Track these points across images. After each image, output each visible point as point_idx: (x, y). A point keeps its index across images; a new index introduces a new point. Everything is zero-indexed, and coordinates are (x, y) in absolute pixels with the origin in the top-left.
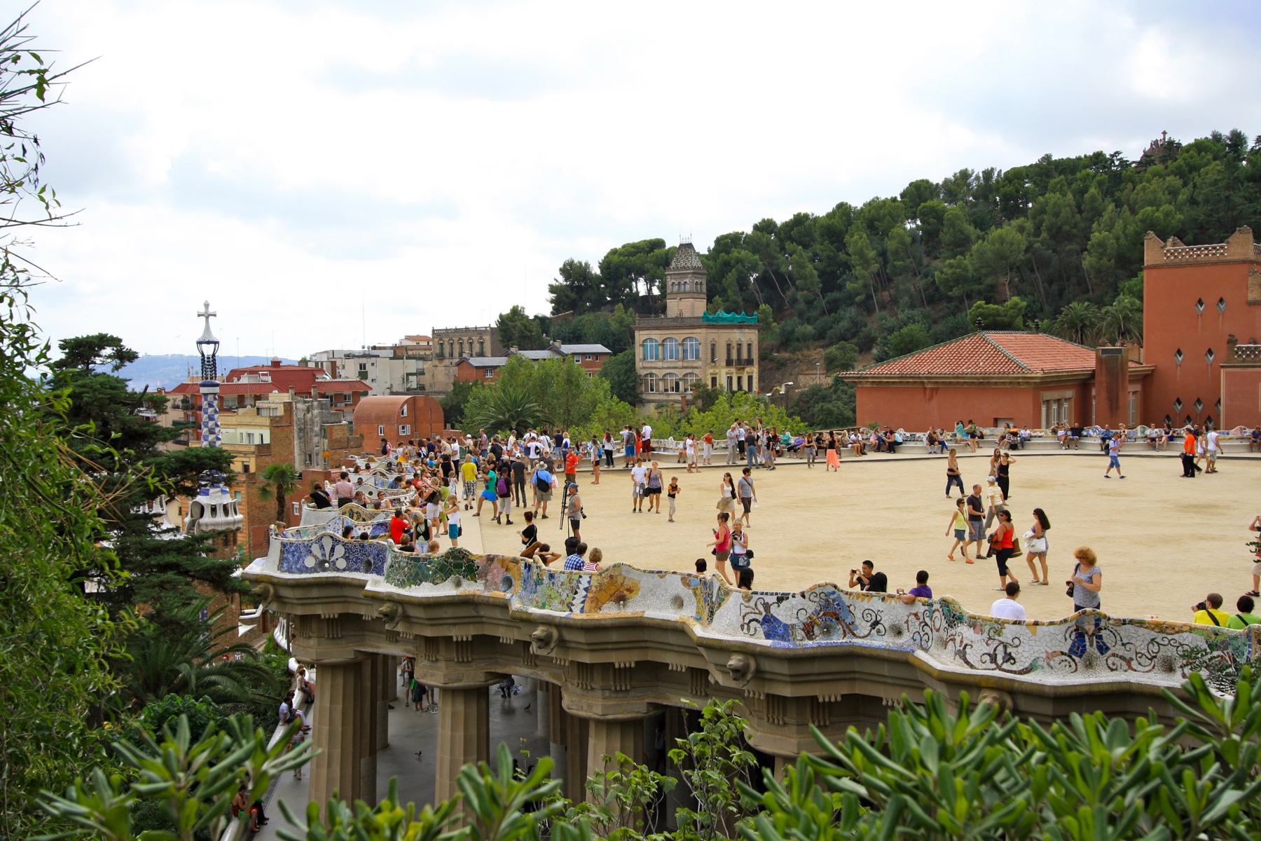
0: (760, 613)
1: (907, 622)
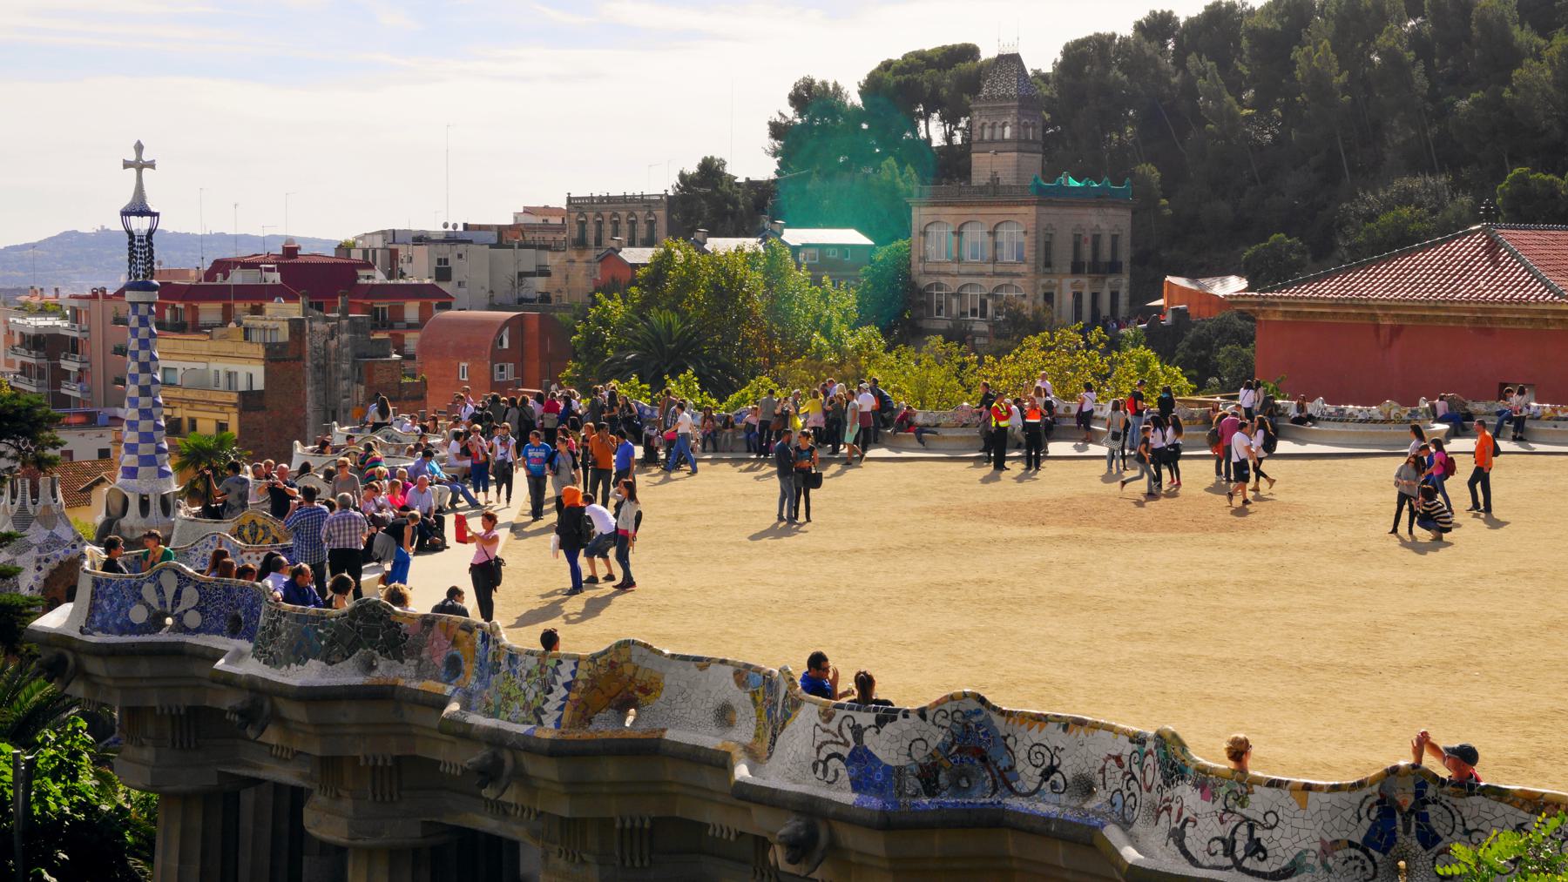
0: (846, 744)
1: (1103, 770)
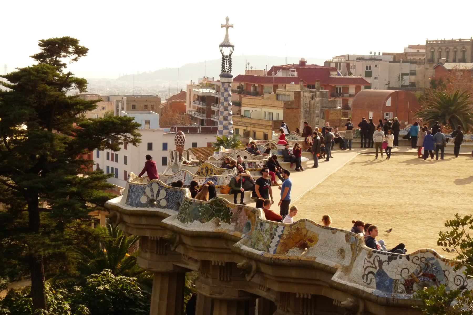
0: (376, 268)
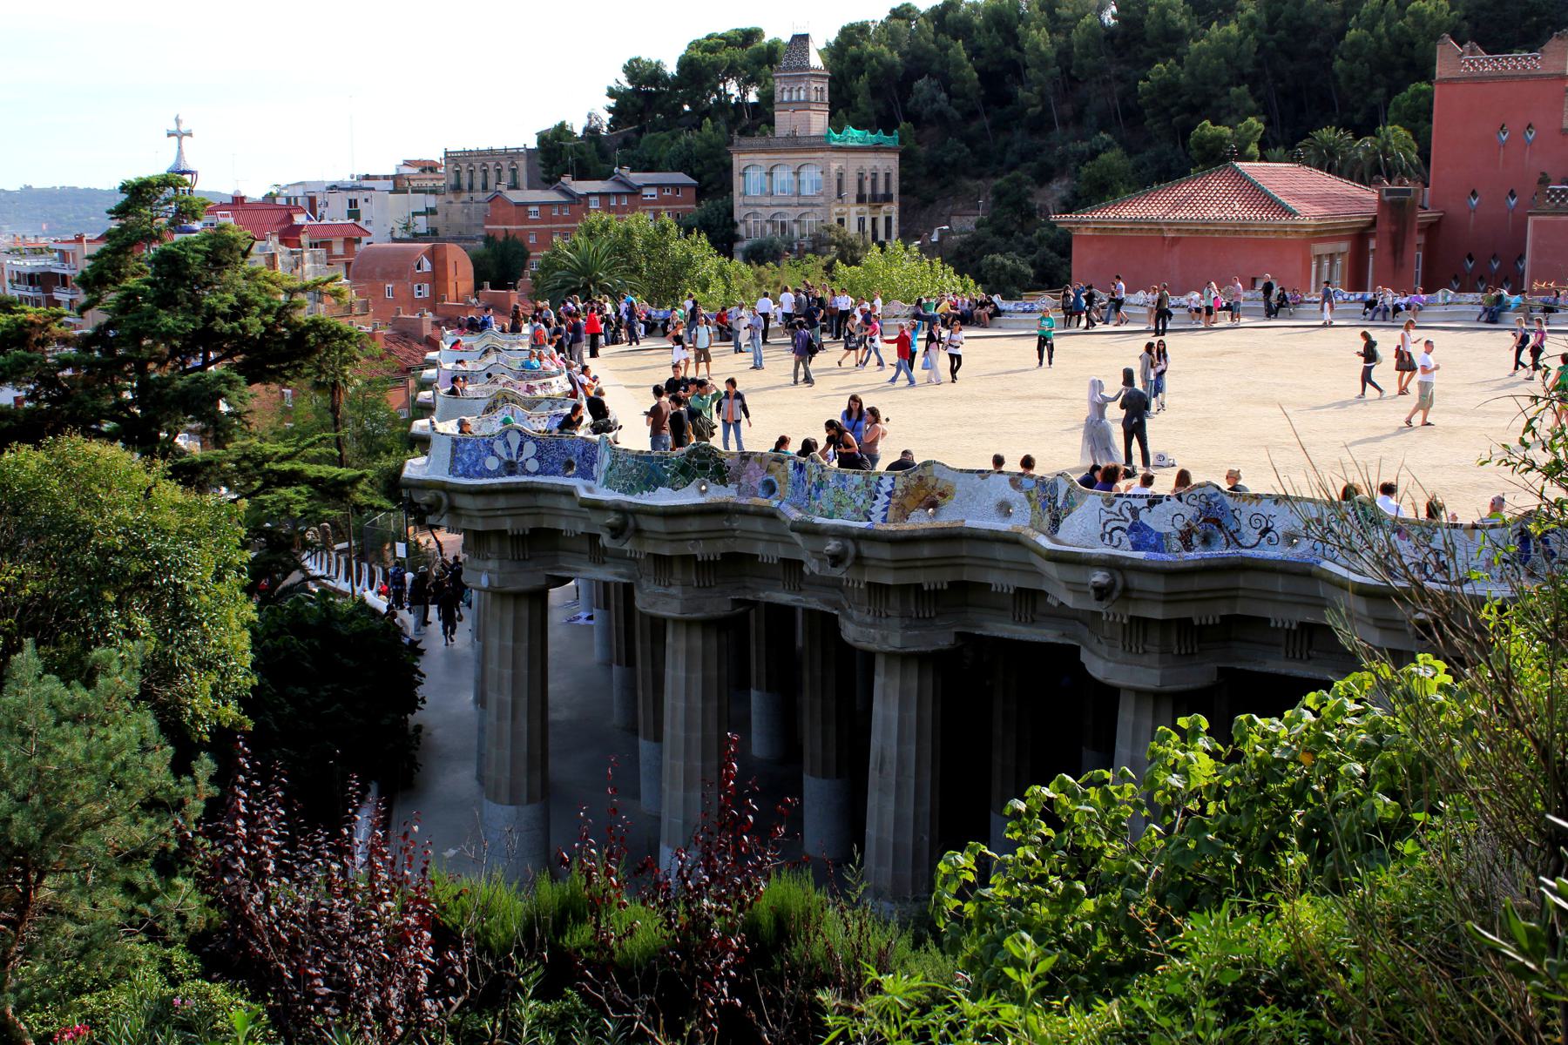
0: (1126, 520)
